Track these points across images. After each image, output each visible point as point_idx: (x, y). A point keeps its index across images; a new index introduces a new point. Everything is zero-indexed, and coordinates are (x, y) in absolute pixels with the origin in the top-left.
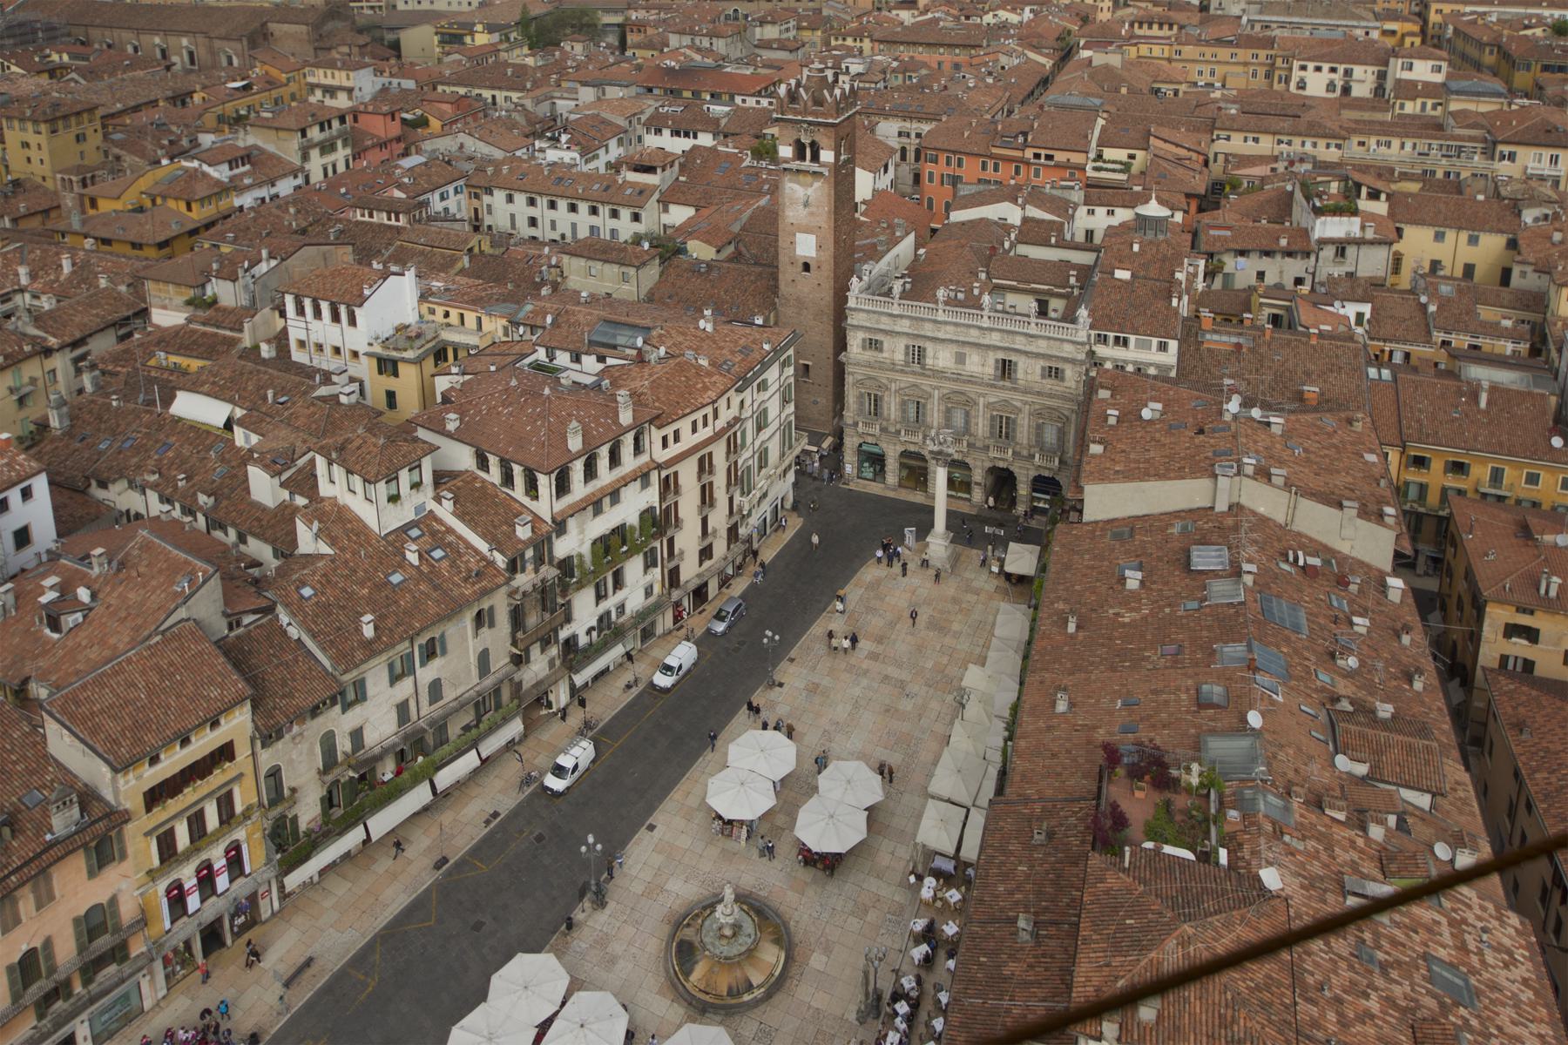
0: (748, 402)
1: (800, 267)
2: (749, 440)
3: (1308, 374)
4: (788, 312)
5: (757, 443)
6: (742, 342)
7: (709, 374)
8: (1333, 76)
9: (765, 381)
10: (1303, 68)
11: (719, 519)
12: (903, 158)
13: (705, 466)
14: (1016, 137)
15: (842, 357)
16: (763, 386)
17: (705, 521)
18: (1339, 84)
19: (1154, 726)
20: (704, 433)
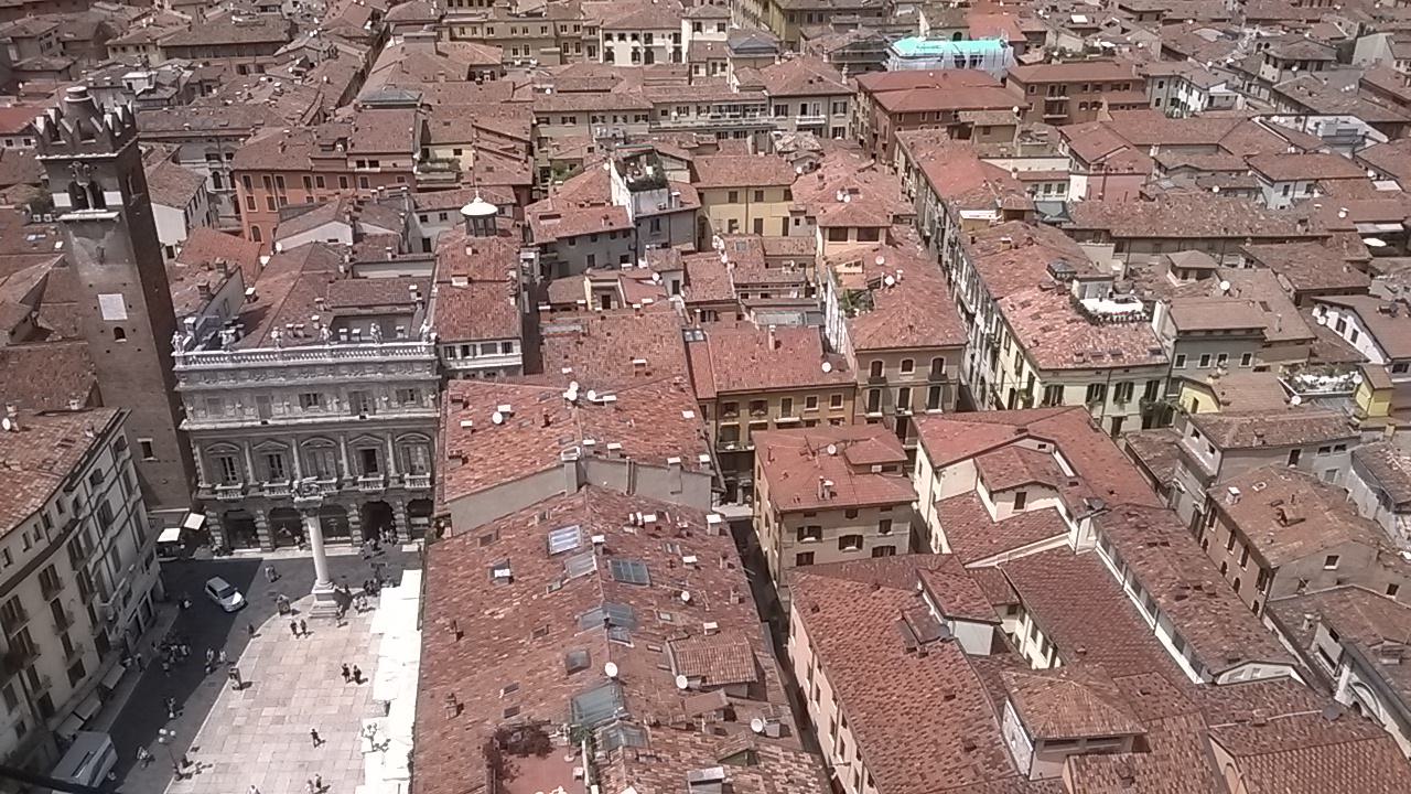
0: (84, 499)
1: (114, 337)
2: (96, 541)
3: (635, 348)
4: (109, 388)
5: (106, 542)
6: (61, 434)
7: (29, 480)
8: (636, 43)
9: (98, 471)
10: (609, 37)
11: (81, 631)
12: (218, 184)
13: (50, 583)
14: (334, 145)
15: (184, 425)
16: (96, 480)
17: (66, 641)
18: (642, 51)
19: (532, 703)
20: (43, 544)
